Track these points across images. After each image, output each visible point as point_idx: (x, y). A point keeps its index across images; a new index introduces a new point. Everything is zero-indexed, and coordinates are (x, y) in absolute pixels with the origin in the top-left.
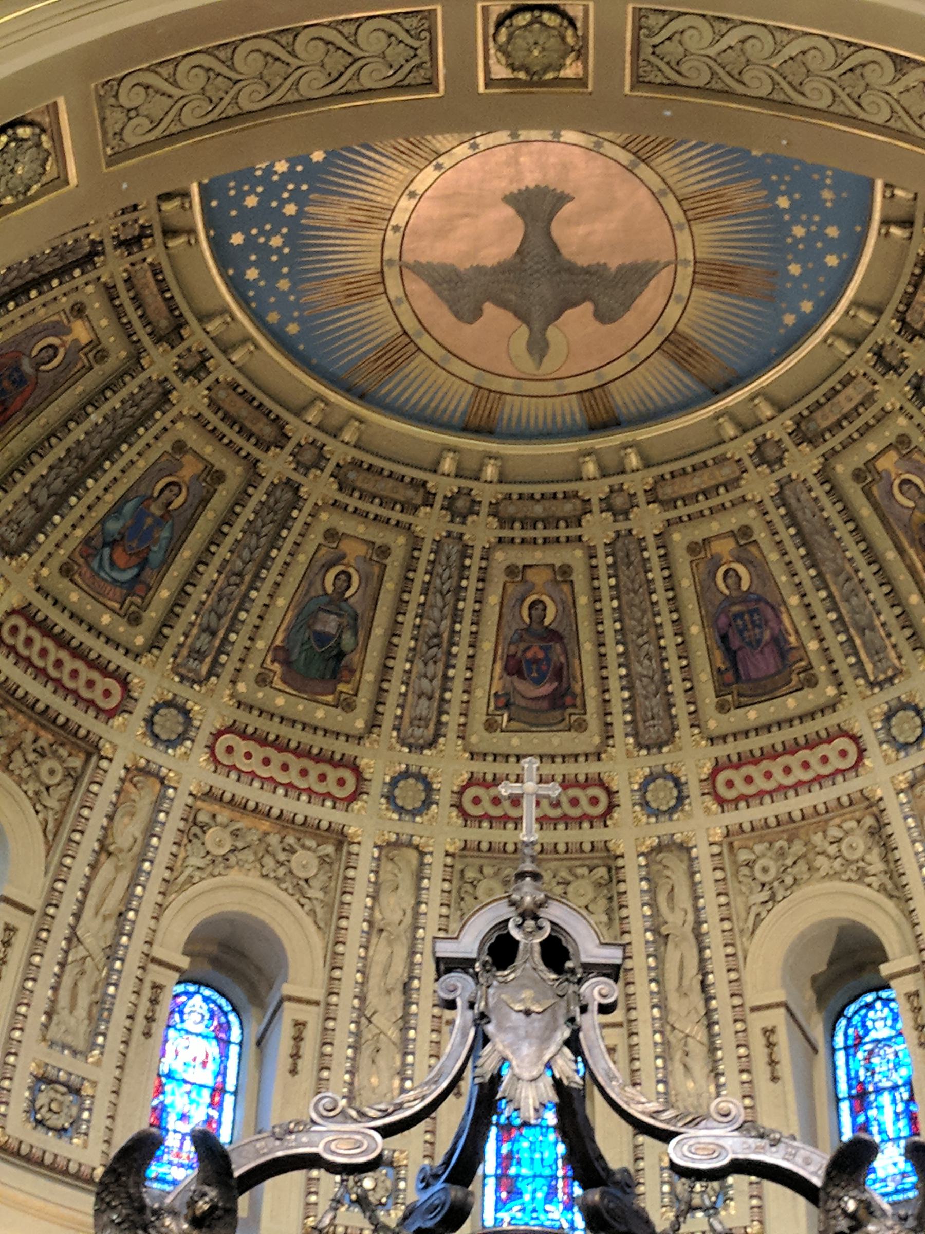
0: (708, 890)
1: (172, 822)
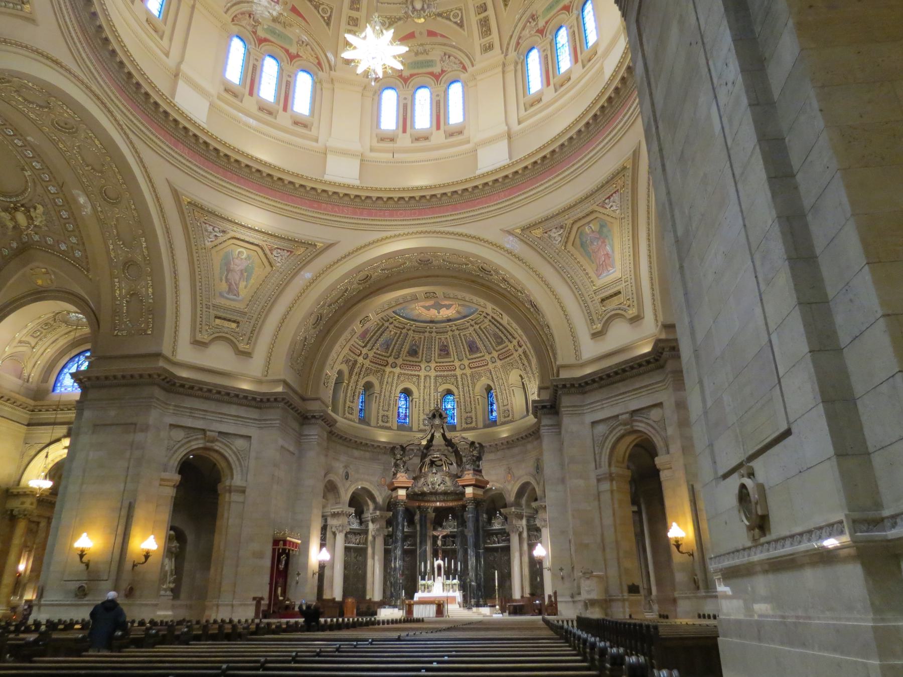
0: (469, 380)
1: (396, 378)
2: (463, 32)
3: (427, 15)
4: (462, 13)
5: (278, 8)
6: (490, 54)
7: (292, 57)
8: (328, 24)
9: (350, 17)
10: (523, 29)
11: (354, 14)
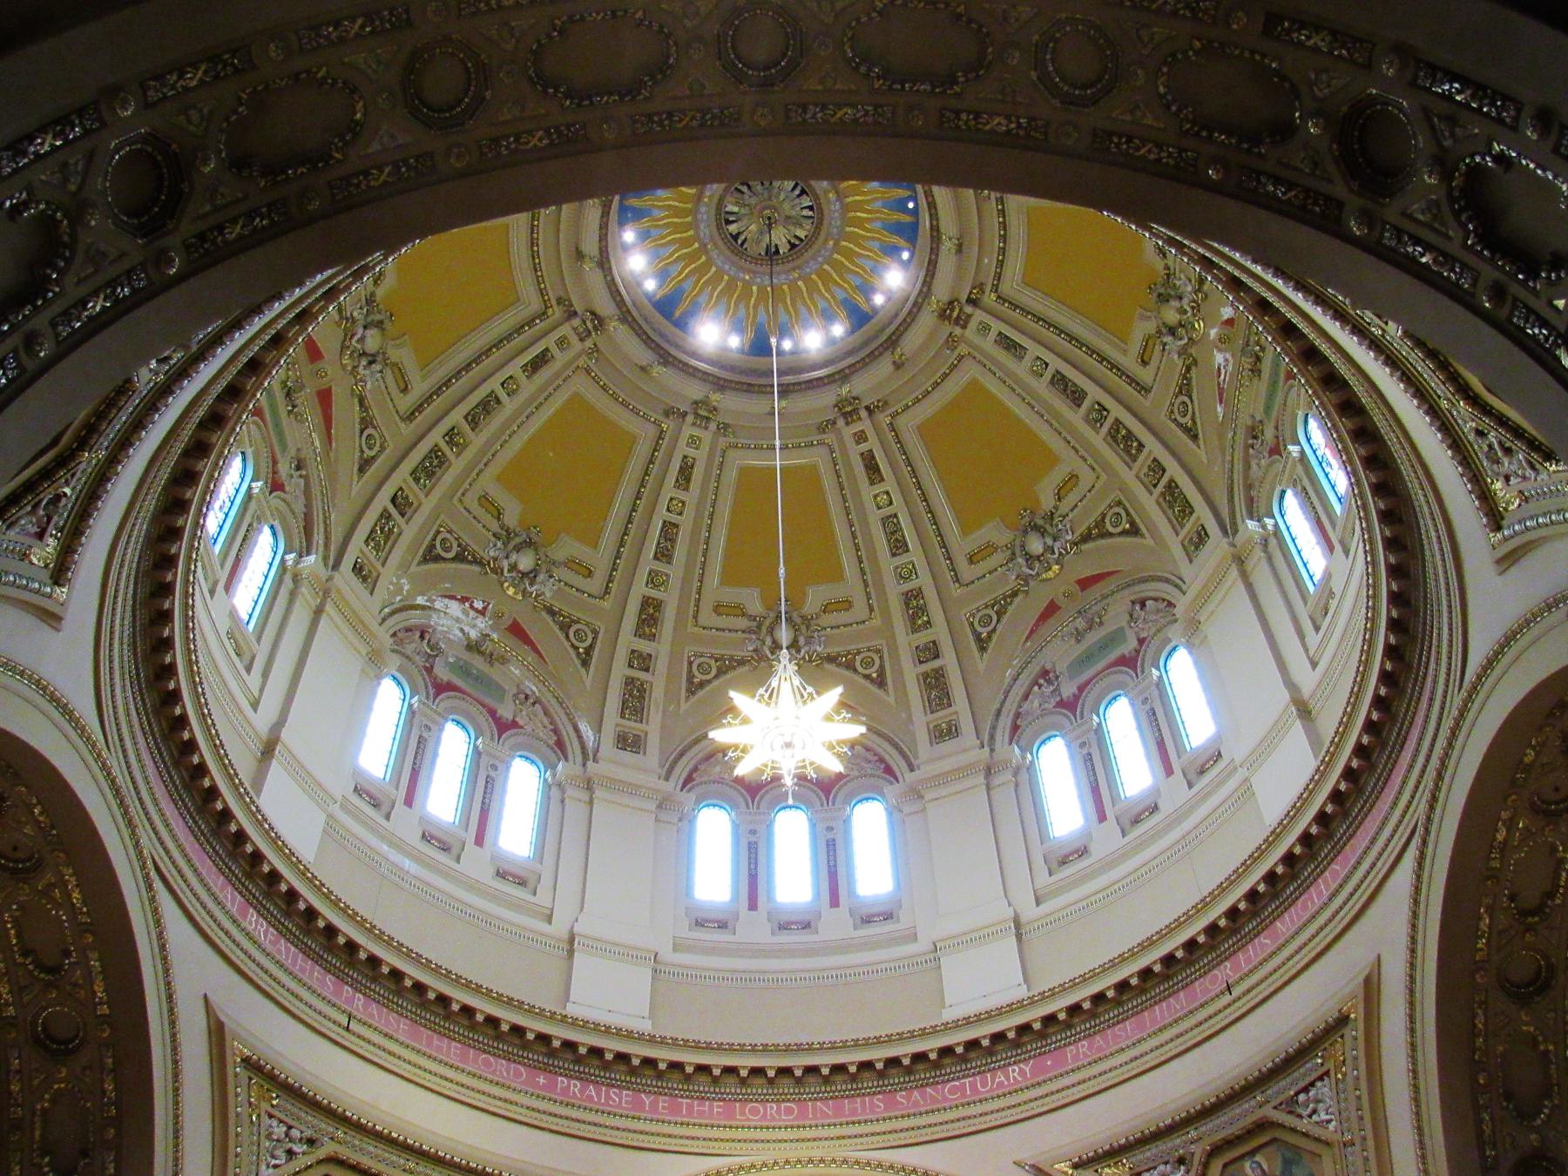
2: (885, 697)
3: (804, 658)
4: (881, 658)
5: (482, 623)
6: (948, 746)
7: (504, 727)
8: (585, 663)
9: (633, 652)
10: (1026, 697)
11: (644, 646)
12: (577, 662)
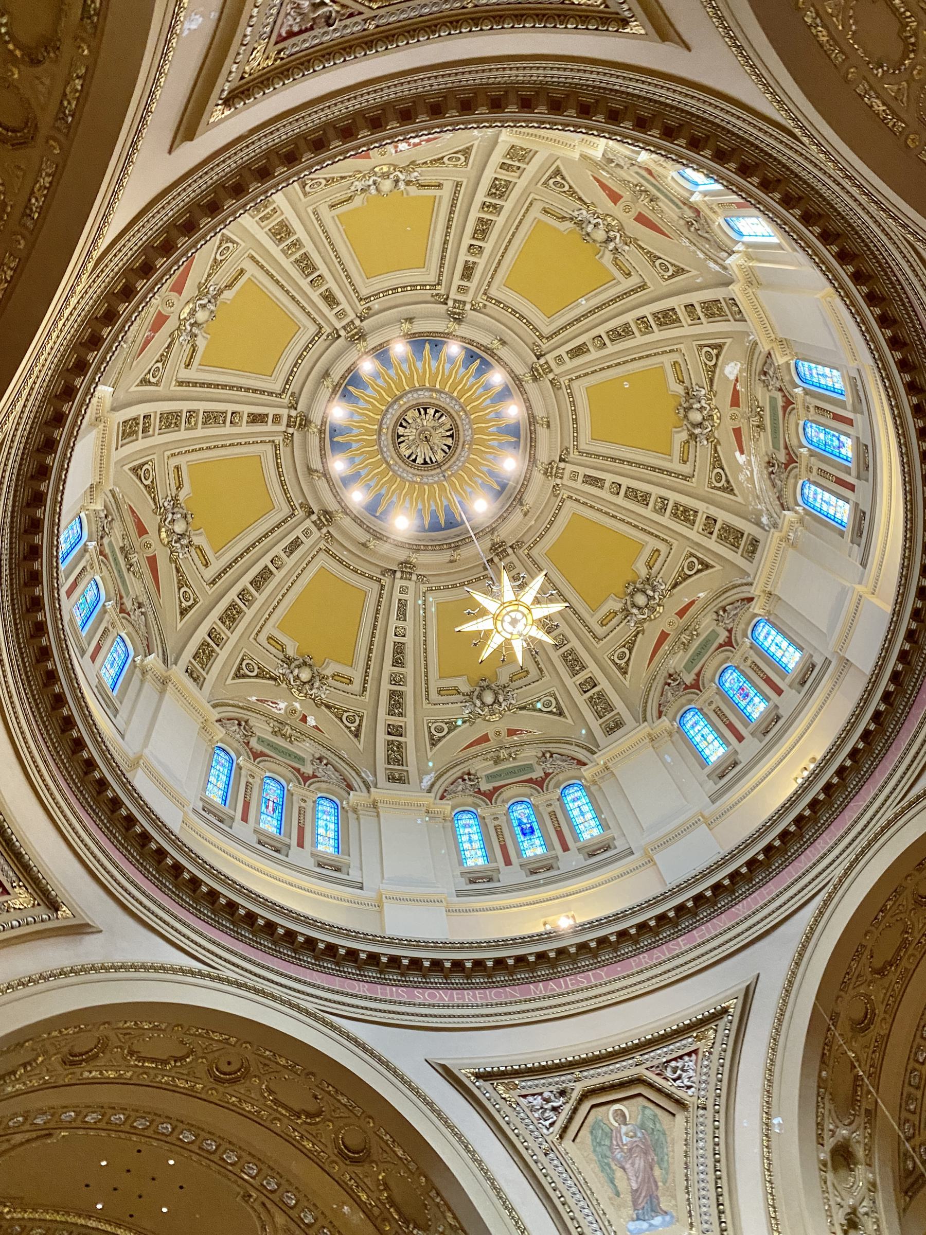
12: (178, 611)
